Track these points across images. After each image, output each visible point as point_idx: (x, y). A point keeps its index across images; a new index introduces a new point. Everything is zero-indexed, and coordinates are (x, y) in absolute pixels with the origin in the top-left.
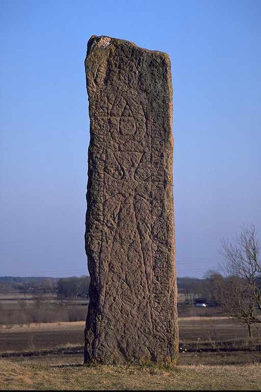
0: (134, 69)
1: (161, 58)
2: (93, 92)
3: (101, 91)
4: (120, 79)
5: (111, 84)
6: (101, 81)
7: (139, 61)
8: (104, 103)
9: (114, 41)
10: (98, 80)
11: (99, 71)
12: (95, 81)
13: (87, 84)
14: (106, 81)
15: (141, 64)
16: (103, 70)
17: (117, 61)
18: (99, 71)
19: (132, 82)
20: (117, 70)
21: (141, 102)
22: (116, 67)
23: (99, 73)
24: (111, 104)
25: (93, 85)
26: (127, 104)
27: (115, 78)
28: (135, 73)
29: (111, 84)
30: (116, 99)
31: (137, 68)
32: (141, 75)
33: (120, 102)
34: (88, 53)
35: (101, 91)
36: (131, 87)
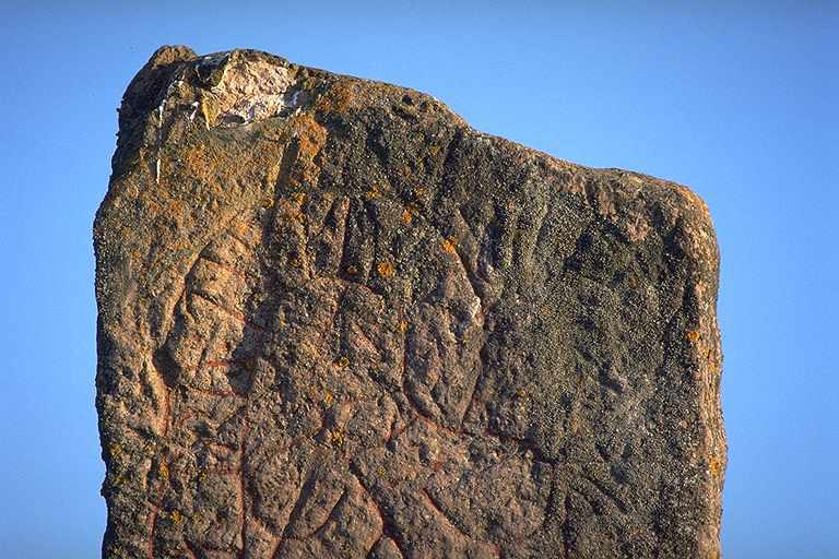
0: (457, 283)
1: (657, 215)
2: (146, 434)
3: (202, 431)
4: (343, 351)
5: (284, 386)
6: (205, 360)
7: (496, 231)
8: (222, 515)
9: (312, 89)
10: (188, 356)
11: (194, 286)
12: (167, 363)
13: (106, 382)
14: (242, 367)
15: (509, 252)
16: (228, 283)
17: (330, 221)
18: (194, 286)
19: (434, 375)
20: (327, 287)
21: (493, 523)
22: (321, 264)
23: (198, 302)
24: (271, 525)
25: (147, 390)
26: (391, 529)
27: (309, 347)
28: (461, 315)
29: (284, 386)
30: (308, 489)
31: (478, 279)
32: (500, 328)
33: (335, 515)
34: (123, 164)
35: (202, 431)
36: (427, 415)
